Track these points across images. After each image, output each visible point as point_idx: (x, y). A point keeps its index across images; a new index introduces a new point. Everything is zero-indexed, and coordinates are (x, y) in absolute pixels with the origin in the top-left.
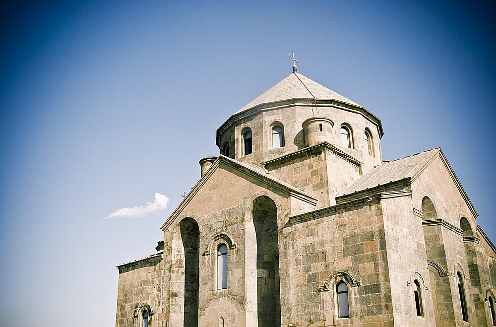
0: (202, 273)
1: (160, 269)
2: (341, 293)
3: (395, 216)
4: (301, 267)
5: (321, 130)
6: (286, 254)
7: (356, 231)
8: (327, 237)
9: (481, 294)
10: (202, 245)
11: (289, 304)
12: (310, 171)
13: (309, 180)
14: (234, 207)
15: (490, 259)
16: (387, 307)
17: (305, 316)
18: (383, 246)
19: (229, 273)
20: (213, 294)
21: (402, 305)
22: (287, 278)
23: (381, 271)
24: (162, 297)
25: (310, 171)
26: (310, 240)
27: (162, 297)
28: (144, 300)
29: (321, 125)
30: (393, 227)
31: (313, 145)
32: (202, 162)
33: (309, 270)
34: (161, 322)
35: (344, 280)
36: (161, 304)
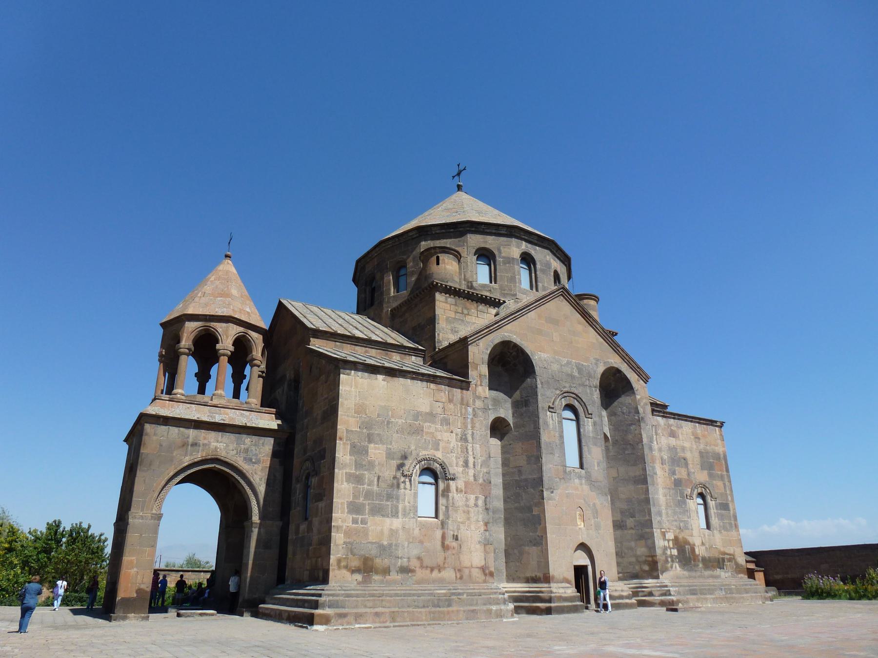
0: (544, 438)
1: (464, 403)
4: (667, 467)
6: (651, 448)
10: (542, 395)
11: (660, 506)
16: (736, 526)
17: (675, 523)
18: (727, 471)
19: (585, 449)
26: (672, 441)
27: (471, 453)
28: (425, 449)
33: (674, 473)
34: (472, 497)
36: (471, 464)
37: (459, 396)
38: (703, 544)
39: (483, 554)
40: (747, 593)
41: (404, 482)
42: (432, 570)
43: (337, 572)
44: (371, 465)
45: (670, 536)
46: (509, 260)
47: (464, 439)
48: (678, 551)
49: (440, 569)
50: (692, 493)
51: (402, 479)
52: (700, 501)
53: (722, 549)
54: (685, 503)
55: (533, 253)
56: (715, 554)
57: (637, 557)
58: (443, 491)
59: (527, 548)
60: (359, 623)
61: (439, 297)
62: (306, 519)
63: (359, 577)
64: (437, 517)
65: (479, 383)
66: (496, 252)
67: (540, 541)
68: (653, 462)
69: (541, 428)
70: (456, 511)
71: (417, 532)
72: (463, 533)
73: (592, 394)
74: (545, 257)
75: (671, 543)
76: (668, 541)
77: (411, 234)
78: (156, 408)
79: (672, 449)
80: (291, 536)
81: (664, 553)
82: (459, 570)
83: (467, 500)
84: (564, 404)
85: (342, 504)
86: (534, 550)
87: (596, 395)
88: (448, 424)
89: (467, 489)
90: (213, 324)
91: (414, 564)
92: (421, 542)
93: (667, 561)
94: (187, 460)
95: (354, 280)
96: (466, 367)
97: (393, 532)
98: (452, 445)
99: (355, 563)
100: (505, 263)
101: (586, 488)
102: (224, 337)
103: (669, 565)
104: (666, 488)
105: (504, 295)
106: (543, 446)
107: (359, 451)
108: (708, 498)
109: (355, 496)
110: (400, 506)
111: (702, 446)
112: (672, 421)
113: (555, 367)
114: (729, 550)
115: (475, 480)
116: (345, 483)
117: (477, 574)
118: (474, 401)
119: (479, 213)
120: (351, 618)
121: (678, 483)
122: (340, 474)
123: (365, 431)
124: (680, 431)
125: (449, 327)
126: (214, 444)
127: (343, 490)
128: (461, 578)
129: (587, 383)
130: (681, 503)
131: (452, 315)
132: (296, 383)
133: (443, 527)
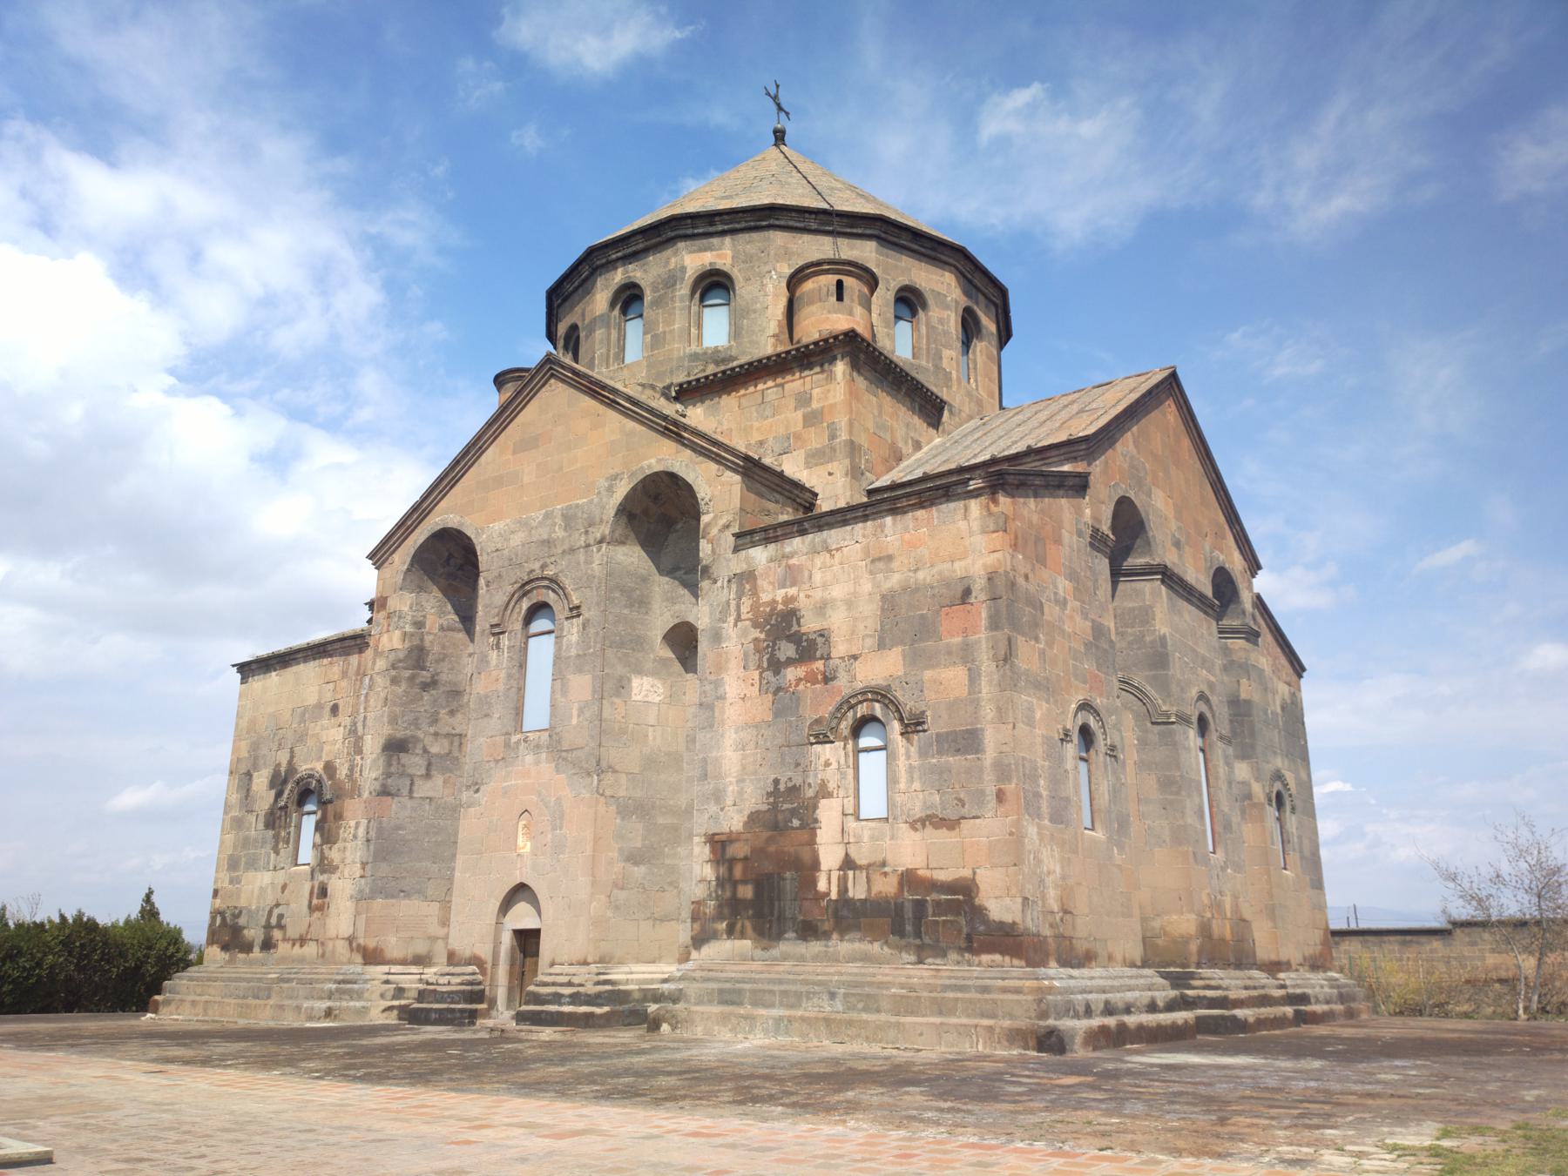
1: (360, 673)
2: (867, 750)
3: (1038, 540)
5: (840, 298)
6: (717, 637)
7: (921, 575)
8: (838, 592)
9: (1257, 779)
10: (486, 606)
12: (800, 414)
13: (798, 437)
15: (1283, 689)
20: (507, 745)
21: (1045, 793)
22: (718, 704)
25: (799, 414)
29: (840, 284)
30: (1029, 567)
31: (816, 336)
32: (500, 380)
34: (352, 823)
35: (878, 709)
38: (848, 864)
40: (941, 1013)
47: (353, 731)
49: (302, 941)
56: (886, 886)
68: (720, 667)
73: (588, 562)
75: (738, 872)
76: (732, 862)
101: (547, 768)
112: (797, 543)
113: (518, 539)
117: (342, 948)
118: (374, 663)
124: (818, 561)
128: (323, 955)
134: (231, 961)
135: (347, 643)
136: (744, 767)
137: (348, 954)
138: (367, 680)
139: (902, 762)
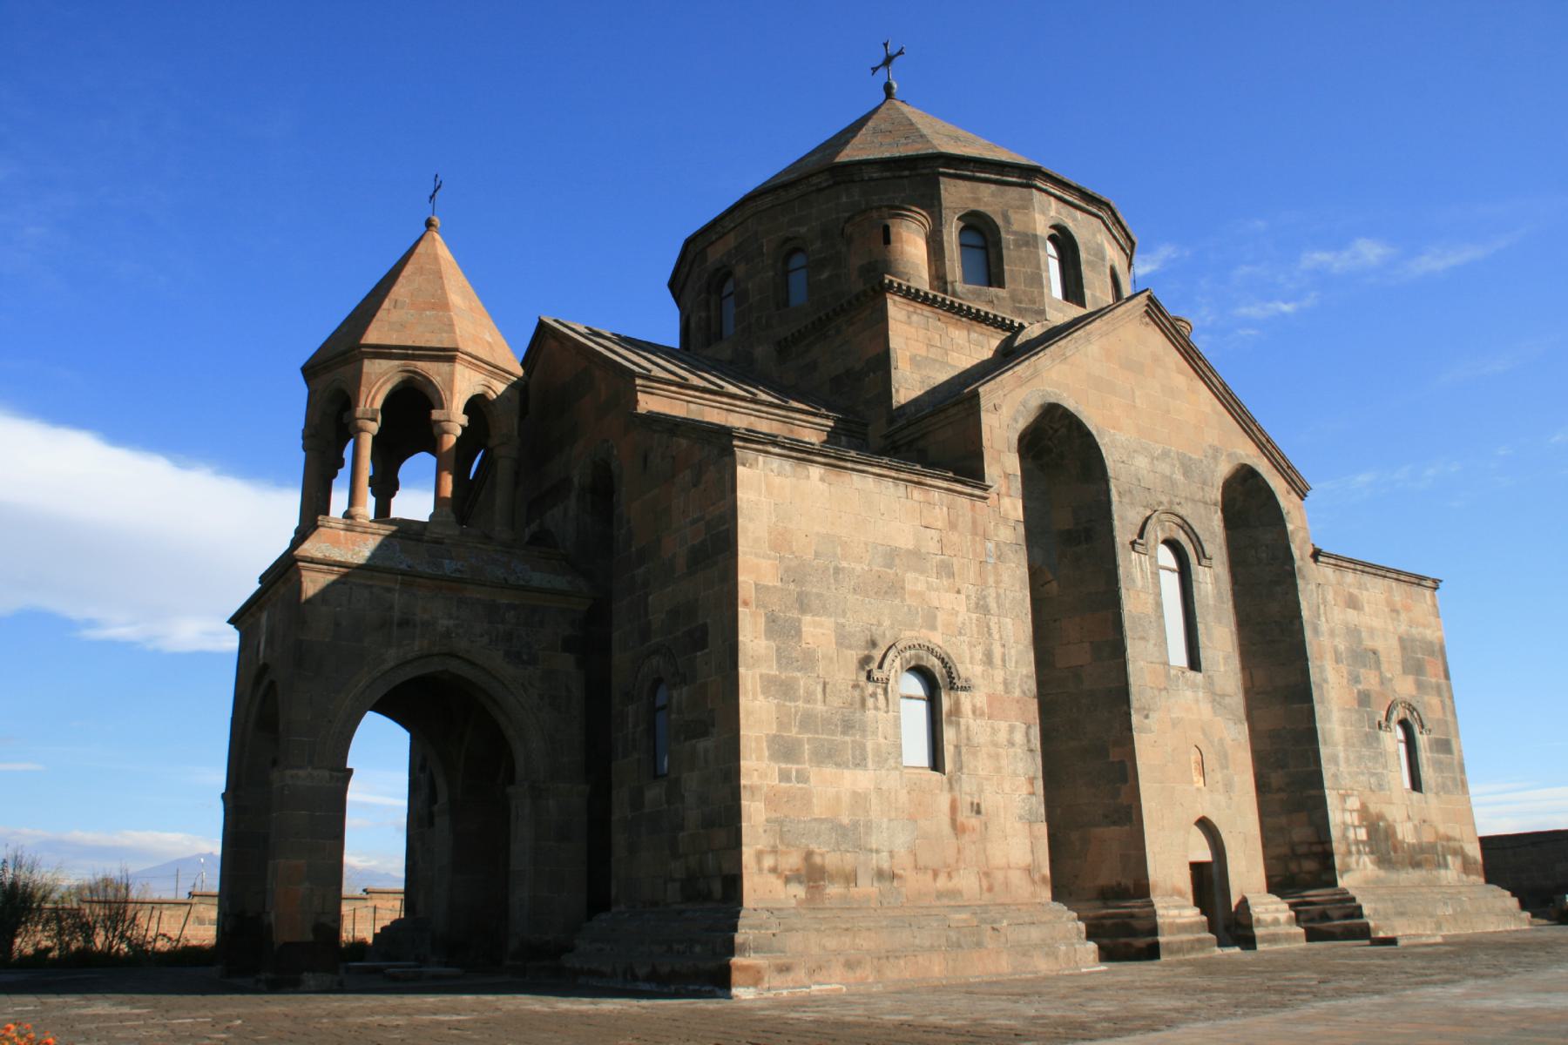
4: (1344, 668)
6: (1316, 631)
11: (1335, 745)
14: (1195, 456)
16: (1464, 784)
17: (1362, 778)
18: (1447, 677)
19: (1201, 627)
23: (1449, 718)
24: (997, 637)
26: (1352, 616)
27: (997, 637)
28: (911, 626)
33: (1356, 679)
34: (1003, 726)
36: (997, 660)
37: (969, 517)
39: (1027, 842)
41: (874, 695)
42: (936, 874)
43: (756, 879)
44: (808, 661)
45: (1353, 803)
46: (1029, 241)
47: (982, 607)
48: (1369, 834)
50: (1388, 718)
51: (870, 688)
52: (1399, 733)
53: (1442, 829)
54: (1377, 739)
55: (1071, 226)
57: (1292, 846)
58: (950, 714)
59: (1098, 831)
60: (819, 983)
61: (896, 309)
62: (656, 776)
63: (799, 891)
64: (936, 763)
65: (1003, 490)
66: (999, 221)
67: (1128, 815)
68: (1322, 658)
69: (1122, 584)
70: (975, 755)
71: (903, 796)
72: (989, 801)
73: (1211, 520)
74: (1094, 235)
77: (815, 180)
78: (323, 546)
79: (1353, 632)
80: (620, 811)
81: (1345, 837)
82: (987, 874)
83: (994, 731)
84: (1161, 537)
85: (758, 739)
86: (1111, 833)
87: (1217, 520)
88: (951, 575)
89: (993, 710)
90: (423, 366)
91: (903, 863)
92: (912, 819)
93: (1350, 853)
94: (392, 656)
95: (677, 285)
96: (979, 456)
97: (859, 799)
98: (960, 619)
99: (793, 861)
100: (1018, 245)
101: (1206, 710)
102: (445, 395)
103: (1353, 859)
104: (1344, 709)
105: (1020, 312)
106: (1127, 624)
107: (782, 629)
108: (1416, 728)
109: (781, 725)
110: (870, 745)
111: (1403, 628)
112: (1350, 577)
113: (1141, 462)
114: (1454, 831)
115: (1007, 691)
116: (761, 697)
117: (1017, 878)
119: (957, 139)
120: (800, 974)
121: (1364, 699)
122: (749, 677)
123: (792, 586)
125: (917, 377)
126: (444, 623)
127: (757, 713)
128: (990, 889)
129: (1199, 496)
130: (1371, 740)
131: (922, 351)
132: (602, 490)
133: (951, 788)
134: (810, 899)
135: (959, 487)
136: (1346, 740)
137: (1030, 888)
138: (990, 545)
139: (1424, 755)
